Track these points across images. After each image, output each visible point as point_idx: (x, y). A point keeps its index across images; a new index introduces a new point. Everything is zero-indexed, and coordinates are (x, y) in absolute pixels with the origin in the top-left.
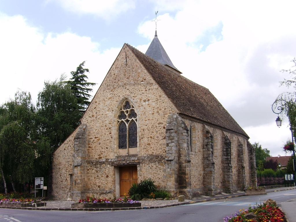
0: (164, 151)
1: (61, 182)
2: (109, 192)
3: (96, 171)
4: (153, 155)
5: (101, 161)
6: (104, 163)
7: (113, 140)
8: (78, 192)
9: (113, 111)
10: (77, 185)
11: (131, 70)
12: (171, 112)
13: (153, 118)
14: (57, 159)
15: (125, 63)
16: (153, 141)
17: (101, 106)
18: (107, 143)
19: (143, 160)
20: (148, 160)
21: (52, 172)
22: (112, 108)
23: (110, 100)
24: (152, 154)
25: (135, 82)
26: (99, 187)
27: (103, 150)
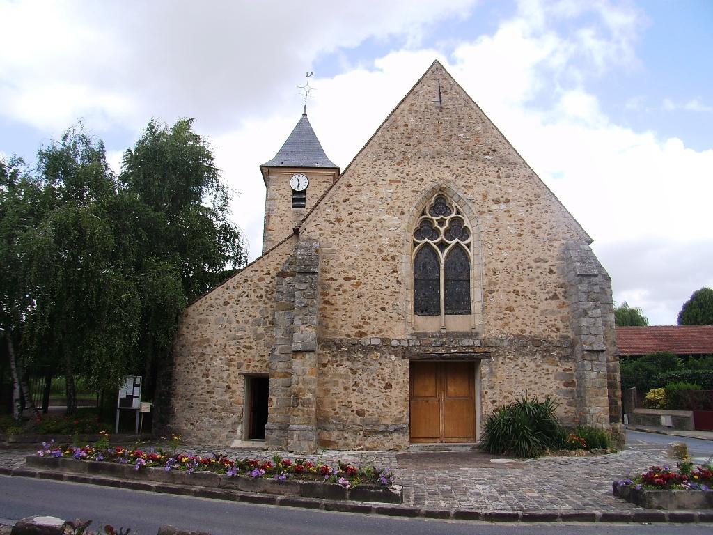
0: (554, 329)
1: (208, 392)
2: (396, 430)
3: (351, 369)
4: (524, 336)
5: (368, 343)
6: (376, 348)
7: (401, 289)
8: (306, 426)
9: (403, 213)
10: (300, 406)
11: (455, 124)
12: (567, 236)
13: (520, 246)
14: (197, 328)
15: (438, 104)
16: (520, 300)
17: (366, 196)
18: (385, 297)
19: (498, 348)
20: (513, 348)
21: (172, 364)
22: (399, 207)
23: (394, 185)
24: (519, 335)
25: (467, 152)
26: (361, 413)
27: (372, 314)
